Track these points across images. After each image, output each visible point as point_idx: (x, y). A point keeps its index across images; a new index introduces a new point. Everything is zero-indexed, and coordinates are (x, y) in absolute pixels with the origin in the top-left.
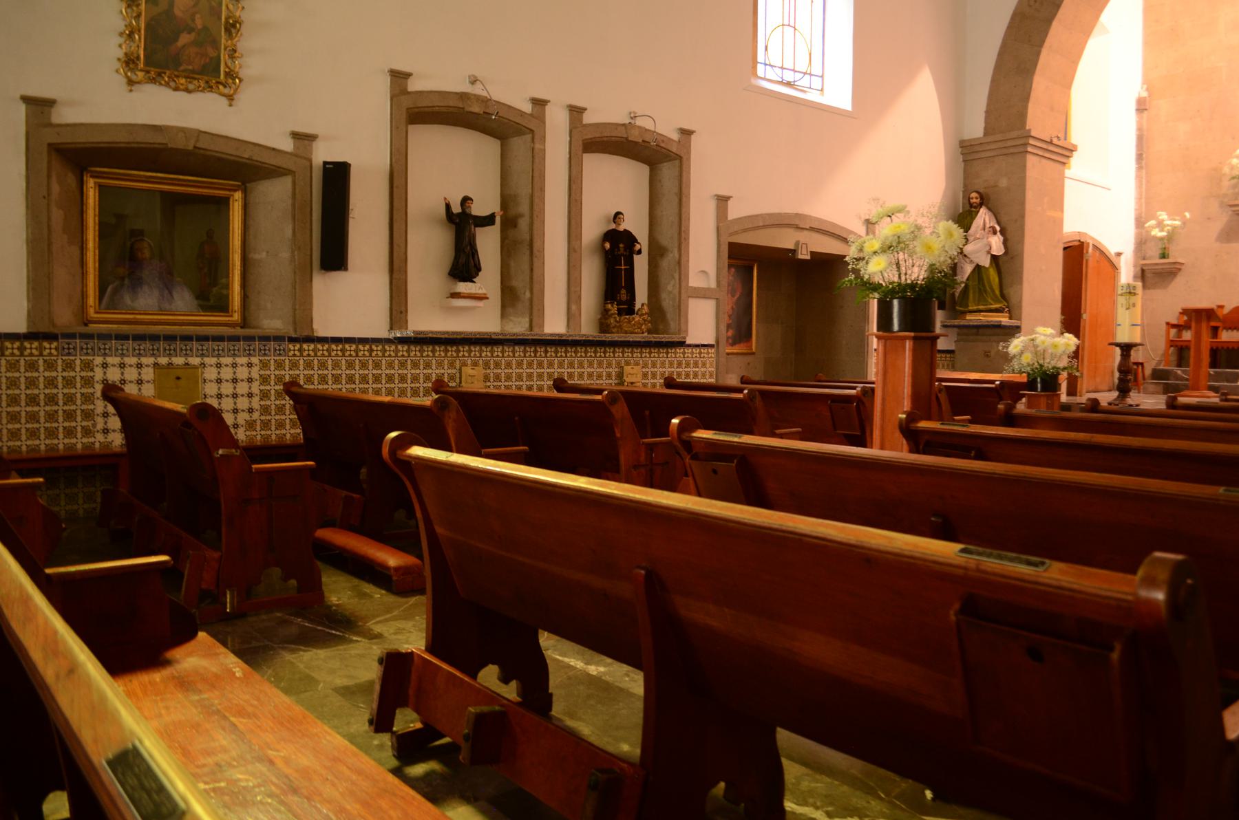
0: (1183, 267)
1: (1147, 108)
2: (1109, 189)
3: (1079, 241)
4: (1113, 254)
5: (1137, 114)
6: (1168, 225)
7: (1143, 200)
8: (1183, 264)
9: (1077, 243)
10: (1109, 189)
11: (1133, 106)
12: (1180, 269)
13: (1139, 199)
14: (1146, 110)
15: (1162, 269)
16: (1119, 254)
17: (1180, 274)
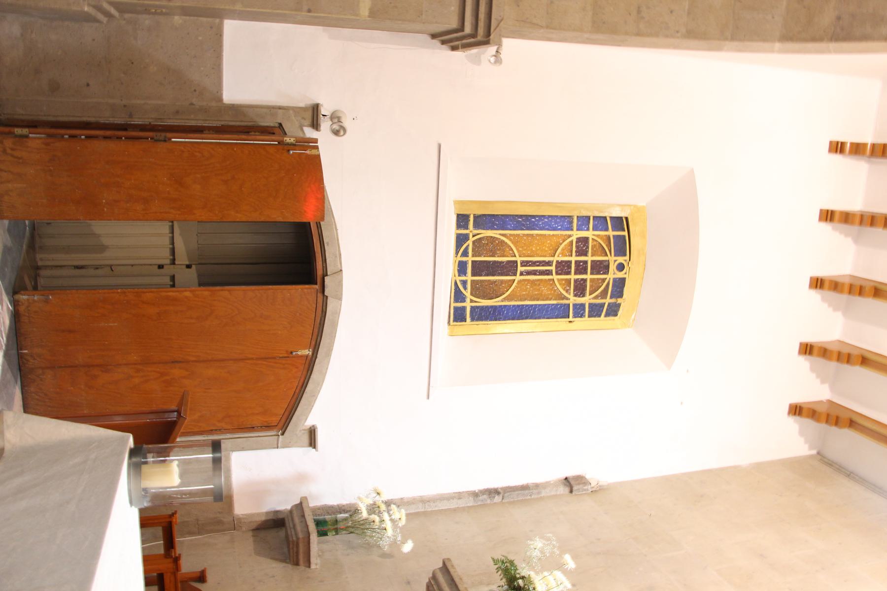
0: (302, 568)
1: (575, 488)
2: (428, 398)
3: (325, 274)
4: (309, 423)
5: (560, 481)
6: (382, 521)
7: (420, 508)
8: (309, 567)
9: (320, 272)
10: (428, 398)
11: (570, 473)
12: (297, 564)
13: (423, 501)
14: (571, 491)
15: (294, 526)
16: (312, 438)
17: (290, 566)
